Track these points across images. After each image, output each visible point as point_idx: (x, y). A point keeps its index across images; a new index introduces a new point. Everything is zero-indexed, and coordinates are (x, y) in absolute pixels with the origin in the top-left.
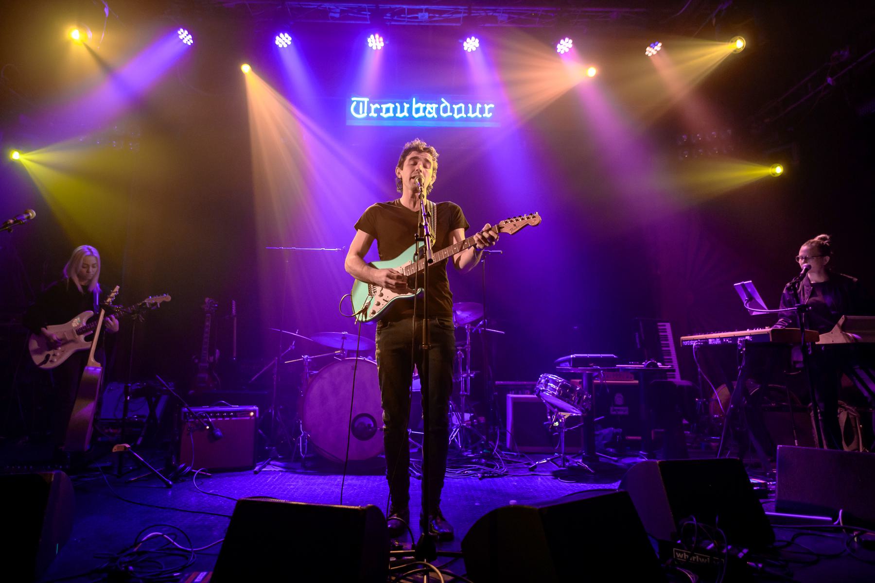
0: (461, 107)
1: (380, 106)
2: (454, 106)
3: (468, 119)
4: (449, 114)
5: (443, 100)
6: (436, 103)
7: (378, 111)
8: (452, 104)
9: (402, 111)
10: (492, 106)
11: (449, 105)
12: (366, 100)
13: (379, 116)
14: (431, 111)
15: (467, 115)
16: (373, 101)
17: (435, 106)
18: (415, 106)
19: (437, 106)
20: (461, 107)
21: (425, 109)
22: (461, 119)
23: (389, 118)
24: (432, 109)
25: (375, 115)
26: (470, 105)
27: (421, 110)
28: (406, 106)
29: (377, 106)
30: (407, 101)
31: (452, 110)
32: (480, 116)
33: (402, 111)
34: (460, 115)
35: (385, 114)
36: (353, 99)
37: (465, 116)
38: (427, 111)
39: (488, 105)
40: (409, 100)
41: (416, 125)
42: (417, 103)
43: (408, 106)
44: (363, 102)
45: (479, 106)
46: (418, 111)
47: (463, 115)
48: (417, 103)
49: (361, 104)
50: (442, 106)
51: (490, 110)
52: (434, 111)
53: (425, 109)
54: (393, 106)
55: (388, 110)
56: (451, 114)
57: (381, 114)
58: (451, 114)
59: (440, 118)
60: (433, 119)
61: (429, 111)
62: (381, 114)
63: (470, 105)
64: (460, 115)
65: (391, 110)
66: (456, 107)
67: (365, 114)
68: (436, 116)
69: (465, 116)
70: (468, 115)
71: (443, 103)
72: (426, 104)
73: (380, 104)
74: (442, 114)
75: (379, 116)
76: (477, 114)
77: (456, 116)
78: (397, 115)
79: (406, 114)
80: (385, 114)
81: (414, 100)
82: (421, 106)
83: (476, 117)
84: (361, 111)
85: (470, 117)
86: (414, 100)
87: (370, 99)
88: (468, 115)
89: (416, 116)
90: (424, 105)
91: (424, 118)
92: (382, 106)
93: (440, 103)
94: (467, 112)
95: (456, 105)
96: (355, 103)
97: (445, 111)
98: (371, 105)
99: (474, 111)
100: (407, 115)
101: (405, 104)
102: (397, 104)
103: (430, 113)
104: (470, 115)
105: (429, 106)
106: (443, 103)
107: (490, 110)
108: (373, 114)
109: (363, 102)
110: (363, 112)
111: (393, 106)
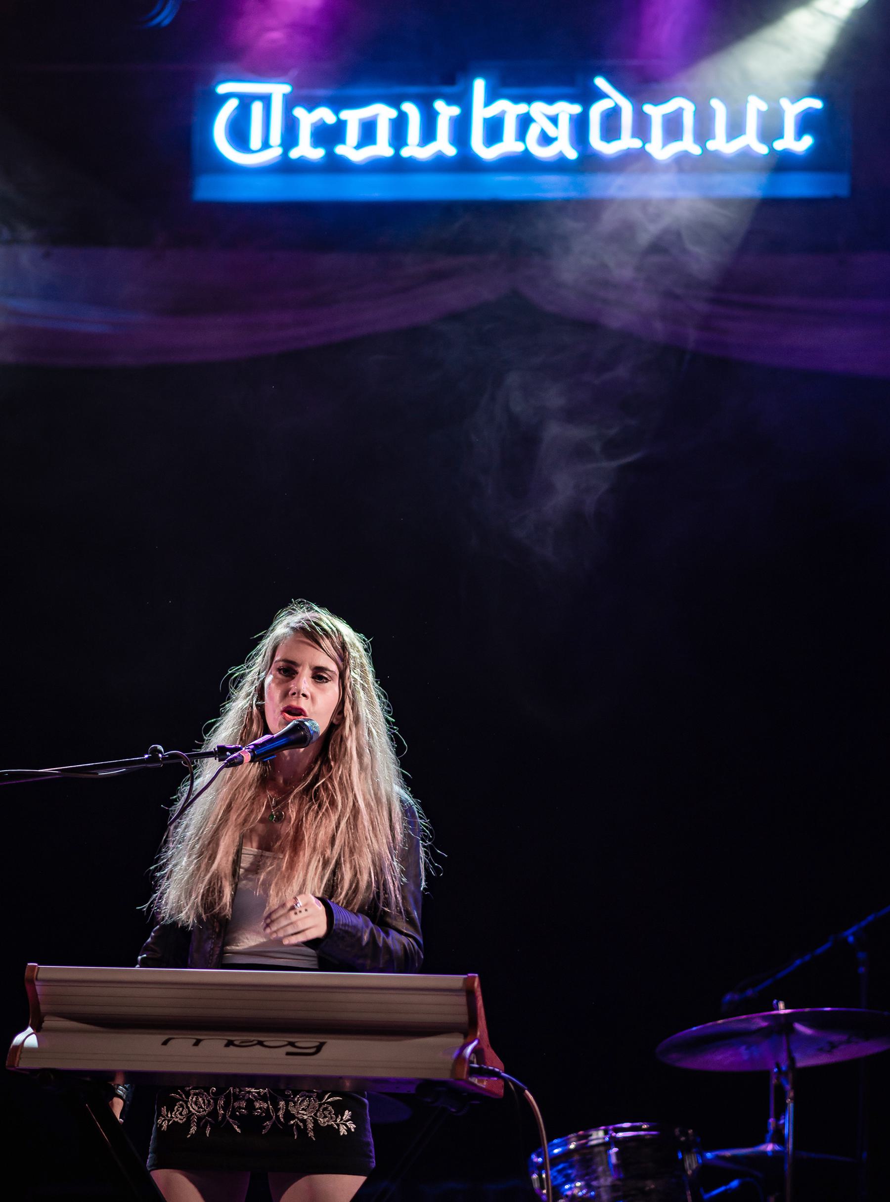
0: (678, 114)
1: (336, 113)
2: (648, 108)
4: (627, 142)
5: (600, 82)
6: (572, 99)
9: (428, 134)
11: (627, 107)
14: (551, 131)
15: (703, 147)
17: (567, 110)
18: (480, 112)
19: (577, 109)
20: (678, 114)
21: (525, 122)
23: (376, 167)
24: (554, 120)
25: (317, 154)
27: (510, 128)
28: (446, 111)
29: (325, 114)
31: (642, 128)
33: (428, 134)
34: (675, 148)
35: (359, 147)
36: (222, 89)
38: (533, 132)
42: (491, 97)
43: (455, 111)
44: (266, 100)
46: (494, 131)
47: (688, 144)
48: (491, 97)
50: (597, 110)
51: (806, 124)
52: (563, 133)
53: (525, 122)
54: (393, 113)
55: (368, 132)
56: (637, 143)
57: (340, 150)
58: (637, 143)
60: (560, 165)
62: (340, 150)
64: (675, 148)
65: (383, 132)
66: (656, 113)
67: (274, 153)
68: (572, 154)
69: (696, 150)
70: (711, 145)
72: (529, 107)
73: (337, 105)
78: (405, 153)
80: (359, 147)
81: (479, 86)
83: (746, 154)
84: (255, 140)
85: (716, 155)
86: (479, 86)
87: (297, 84)
88: (711, 145)
92: (345, 114)
93: (588, 96)
98: (299, 112)
100: (451, 151)
101: (439, 105)
102: (411, 109)
103: (546, 140)
105: (539, 109)
106: (601, 95)
109: (266, 100)
110: (266, 145)
111: (393, 113)
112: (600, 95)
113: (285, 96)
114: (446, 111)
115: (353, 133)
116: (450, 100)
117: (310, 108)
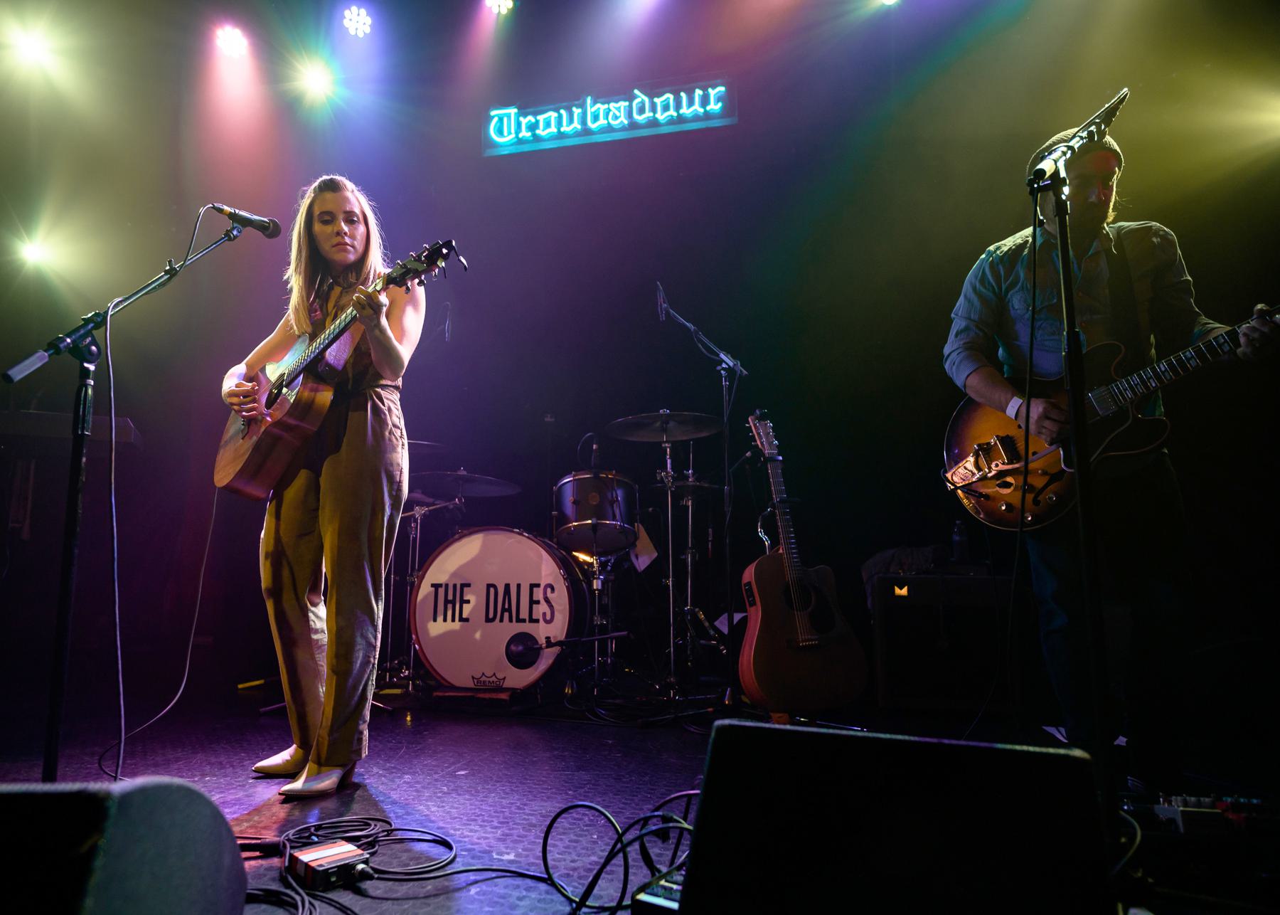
0: (668, 98)
1: (536, 119)
2: (656, 100)
3: (681, 119)
4: (648, 114)
5: (636, 92)
6: (625, 100)
7: (533, 127)
8: (651, 96)
9: (571, 120)
10: (721, 89)
11: (647, 100)
12: (513, 111)
13: (534, 135)
14: (618, 114)
15: (678, 112)
16: (523, 111)
18: (590, 110)
19: (627, 103)
22: (671, 122)
24: (619, 109)
26: (683, 94)
27: (601, 116)
28: (577, 111)
29: (530, 118)
30: (576, 103)
31: (653, 108)
32: (701, 110)
33: (571, 120)
37: (675, 114)
38: (611, 114)
39: (714, 87)
40: (581, 101)
41: (593, 141)
42: (595, 102)
45: (698, 93)
46: (596, 118)
47: (672, 112)
49: (505, 119)
50: (635, 103)
51: (719, 99)
55: (548, 125)
56: (652, 114)
57: (537, 132)
59: (633, 125)
60: (623, 129)
61: (614, 114)
62: (537, 132)
63: (683, 94)
64: (667, 114)
67: (513, 135)
70: (681, 111)
71: (639, 97)
73: (535, 114)
74: (636, 117)
75: (534, 135)
76: (697, 108)
77: (661, 117)
78: (562, 130)
79: (577, 125)
81: (589, 100)
82: (601, 107)
84: (505, 131)
86: (589, 100)
87: (519, 108)
88: (681, 111)
89: (593, 126)
90: (606, 106)
91: (610, 129)
93: (631, 98)
94: (678, 106)
95: (658, 97)
96: (495, 120)
97: (641, 110)
99: (691, 103)
101: (574, 109)
102: (562, 111)
103: (616, 118)
104: (686, 111)
105: (613, 105)
106: (639, 97)
107: (719, 99)
108: (525, 134)
112: (635, 97)
113: (515, 114)
114: (577, 111)
115: (541, 125)
116: (578, 107)
117: (525, 115)
